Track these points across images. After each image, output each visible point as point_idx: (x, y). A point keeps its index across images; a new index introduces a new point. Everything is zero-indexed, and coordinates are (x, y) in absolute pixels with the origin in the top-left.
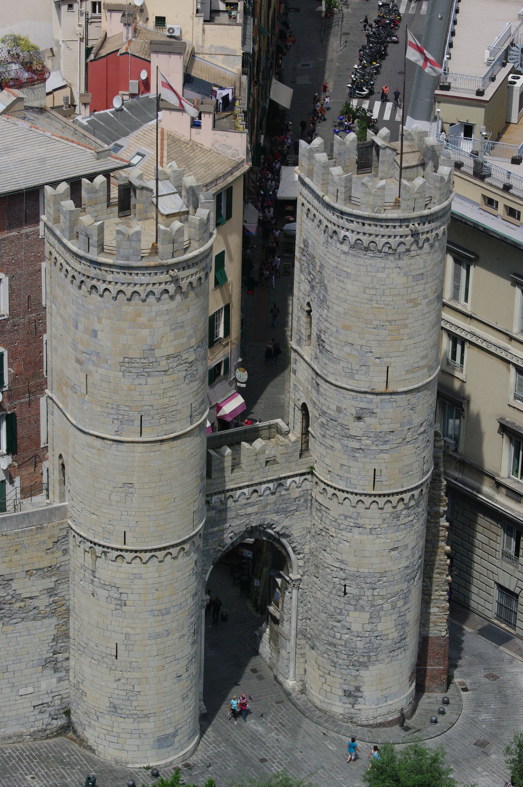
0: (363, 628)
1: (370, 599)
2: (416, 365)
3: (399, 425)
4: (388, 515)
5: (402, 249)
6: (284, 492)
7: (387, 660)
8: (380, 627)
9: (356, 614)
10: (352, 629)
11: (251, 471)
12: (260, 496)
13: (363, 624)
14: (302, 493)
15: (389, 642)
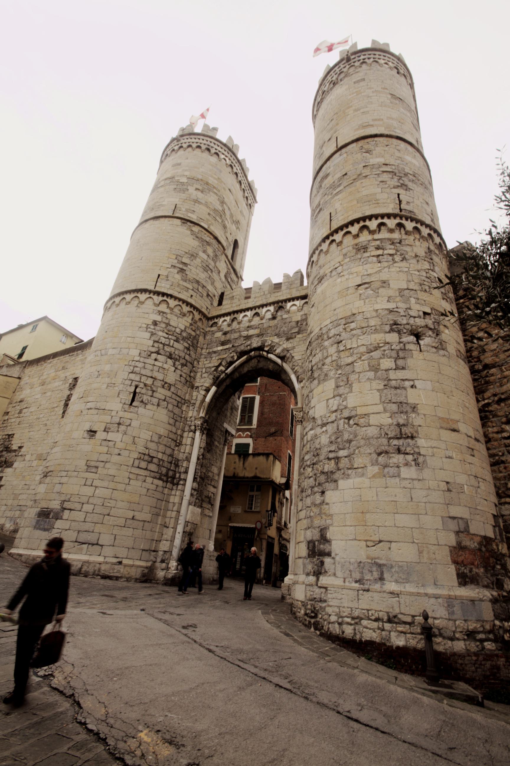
0: (328, 406)
1: (334, 358)
2: (367, 124)
3: (351, 166)
4: (351, 248)
5: (342, 75)
6: (285, 316)
7: (374, 470)
8: (352, 401)
9: (320, 388)
10: (316, 417)
11: (255, 298)
12: (262, 319)
13: (327, 400)
14: (304, 317)
15: (372, 431)
